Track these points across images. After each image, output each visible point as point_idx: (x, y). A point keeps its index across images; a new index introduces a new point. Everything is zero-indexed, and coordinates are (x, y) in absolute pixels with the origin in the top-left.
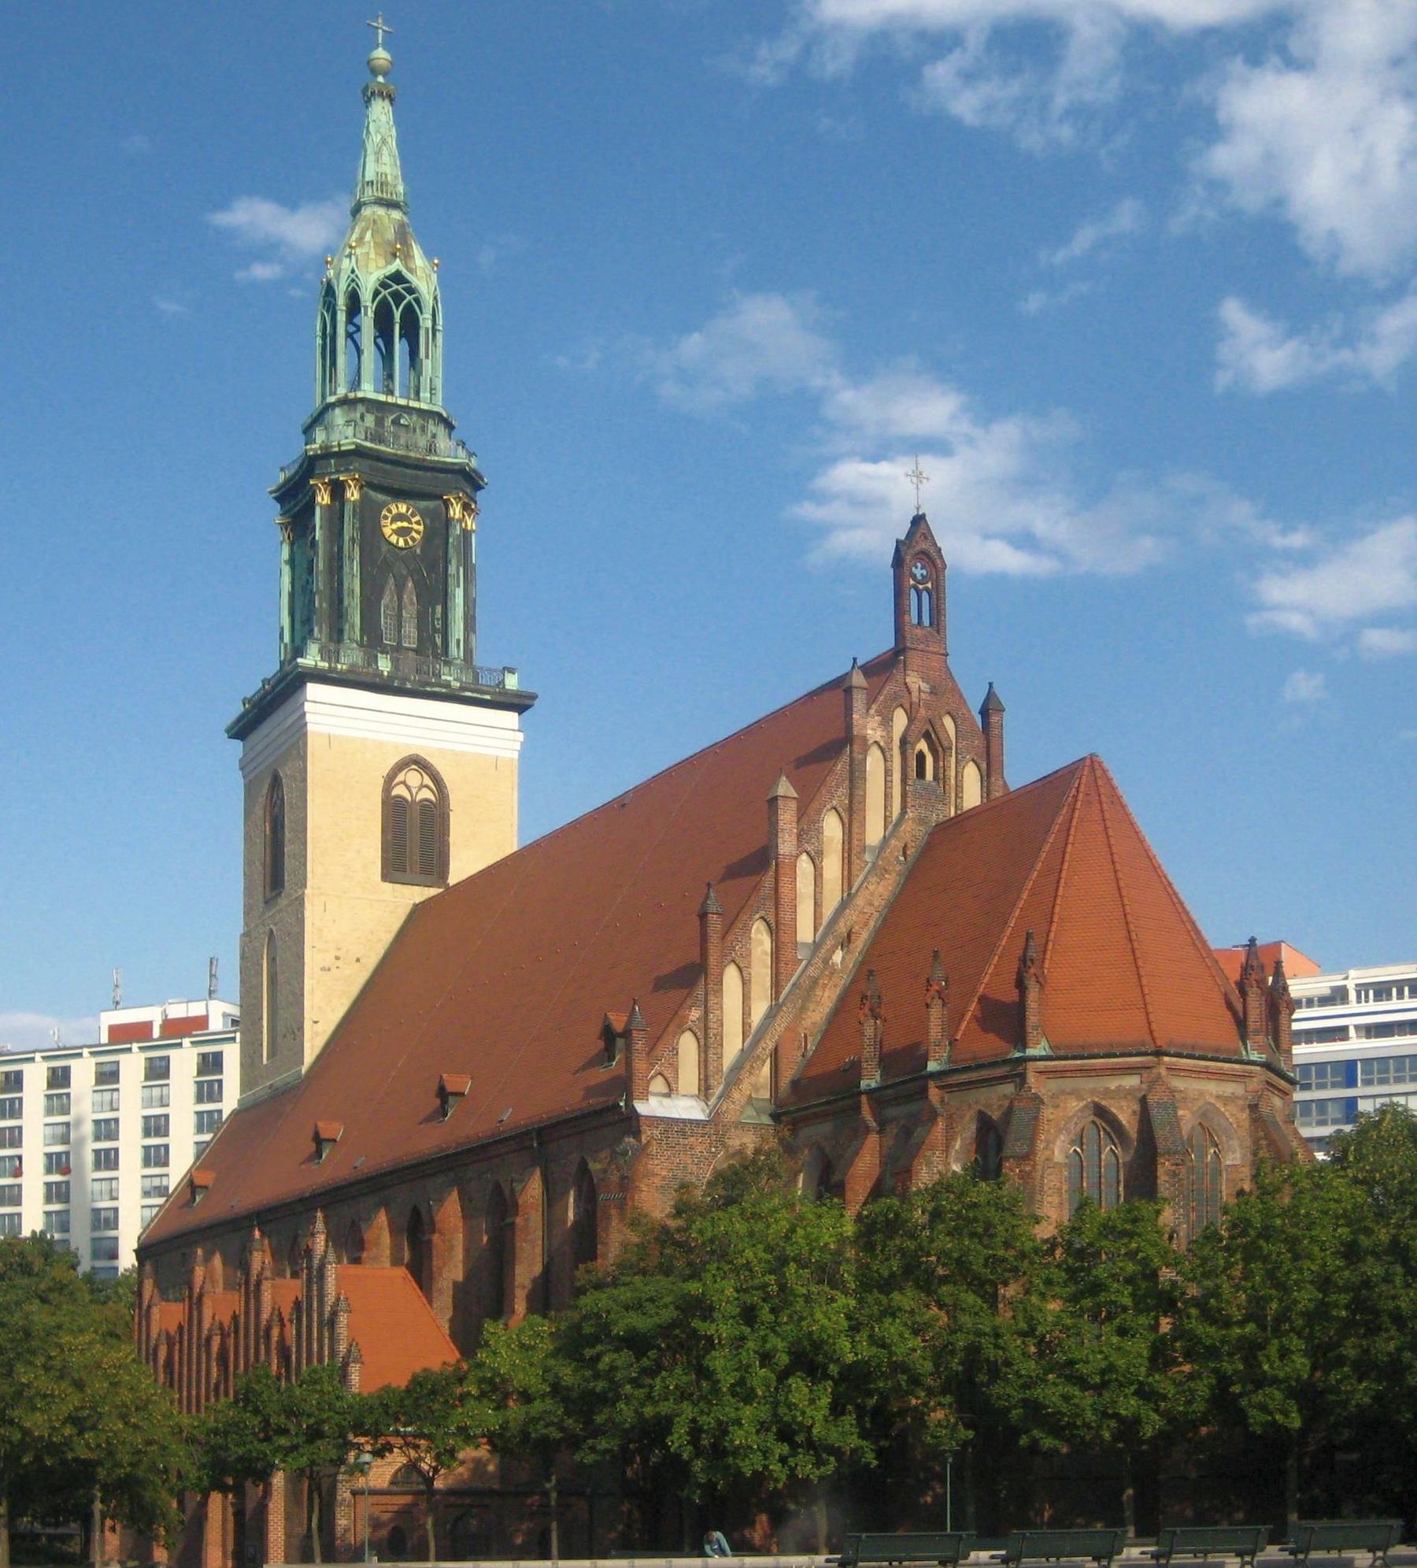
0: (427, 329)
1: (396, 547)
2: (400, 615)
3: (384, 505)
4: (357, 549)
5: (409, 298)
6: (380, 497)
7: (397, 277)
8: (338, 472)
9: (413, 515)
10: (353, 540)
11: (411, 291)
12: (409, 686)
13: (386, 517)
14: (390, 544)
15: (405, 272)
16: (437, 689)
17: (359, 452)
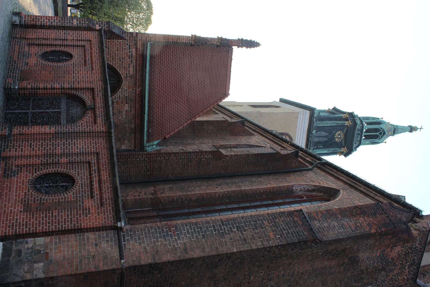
0: (375, 141)
1: (335, 135)
2: (320, 137)
3: (343, 131)
4: (336, 125)
5: (381, 136)
6: (345, 131)
7: (384, 133)
8: (350, 119)
9: (341, 139)
10: (338, 124)
11: (382, 137)
12: (310, 138)
13: (341, 132)
14: (335, 133)
15: (385, 135)
16: (309, 146)
17: (355, 124)
